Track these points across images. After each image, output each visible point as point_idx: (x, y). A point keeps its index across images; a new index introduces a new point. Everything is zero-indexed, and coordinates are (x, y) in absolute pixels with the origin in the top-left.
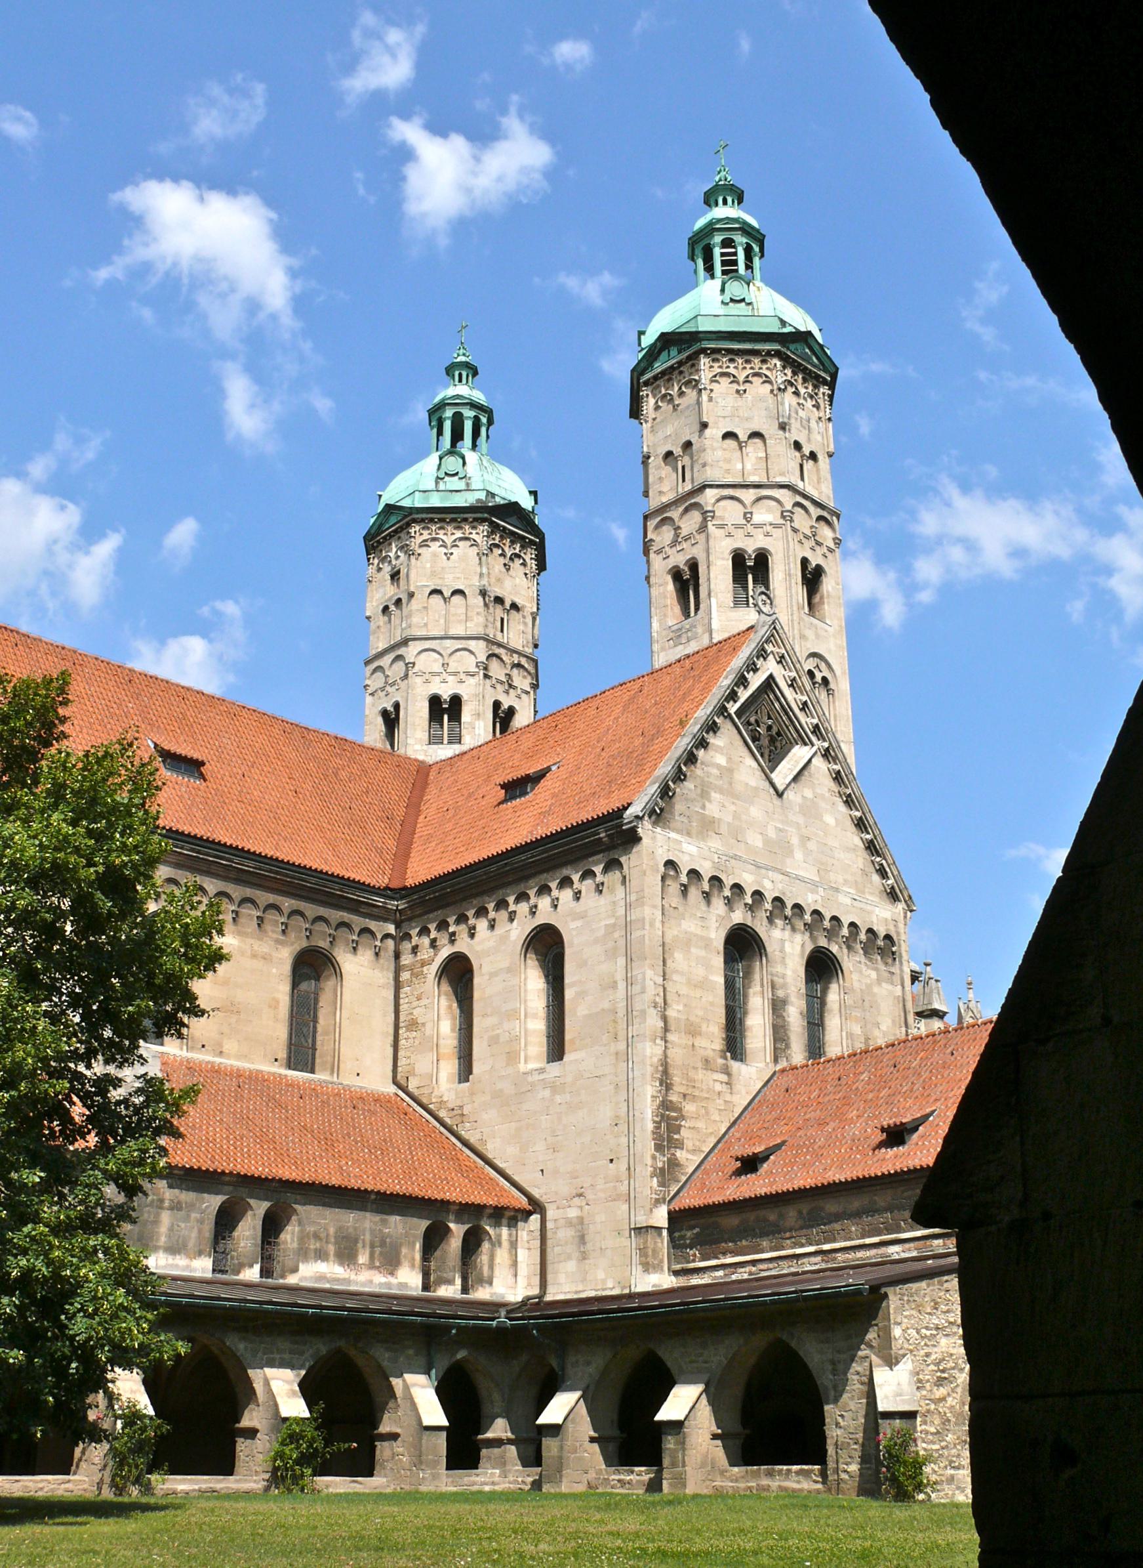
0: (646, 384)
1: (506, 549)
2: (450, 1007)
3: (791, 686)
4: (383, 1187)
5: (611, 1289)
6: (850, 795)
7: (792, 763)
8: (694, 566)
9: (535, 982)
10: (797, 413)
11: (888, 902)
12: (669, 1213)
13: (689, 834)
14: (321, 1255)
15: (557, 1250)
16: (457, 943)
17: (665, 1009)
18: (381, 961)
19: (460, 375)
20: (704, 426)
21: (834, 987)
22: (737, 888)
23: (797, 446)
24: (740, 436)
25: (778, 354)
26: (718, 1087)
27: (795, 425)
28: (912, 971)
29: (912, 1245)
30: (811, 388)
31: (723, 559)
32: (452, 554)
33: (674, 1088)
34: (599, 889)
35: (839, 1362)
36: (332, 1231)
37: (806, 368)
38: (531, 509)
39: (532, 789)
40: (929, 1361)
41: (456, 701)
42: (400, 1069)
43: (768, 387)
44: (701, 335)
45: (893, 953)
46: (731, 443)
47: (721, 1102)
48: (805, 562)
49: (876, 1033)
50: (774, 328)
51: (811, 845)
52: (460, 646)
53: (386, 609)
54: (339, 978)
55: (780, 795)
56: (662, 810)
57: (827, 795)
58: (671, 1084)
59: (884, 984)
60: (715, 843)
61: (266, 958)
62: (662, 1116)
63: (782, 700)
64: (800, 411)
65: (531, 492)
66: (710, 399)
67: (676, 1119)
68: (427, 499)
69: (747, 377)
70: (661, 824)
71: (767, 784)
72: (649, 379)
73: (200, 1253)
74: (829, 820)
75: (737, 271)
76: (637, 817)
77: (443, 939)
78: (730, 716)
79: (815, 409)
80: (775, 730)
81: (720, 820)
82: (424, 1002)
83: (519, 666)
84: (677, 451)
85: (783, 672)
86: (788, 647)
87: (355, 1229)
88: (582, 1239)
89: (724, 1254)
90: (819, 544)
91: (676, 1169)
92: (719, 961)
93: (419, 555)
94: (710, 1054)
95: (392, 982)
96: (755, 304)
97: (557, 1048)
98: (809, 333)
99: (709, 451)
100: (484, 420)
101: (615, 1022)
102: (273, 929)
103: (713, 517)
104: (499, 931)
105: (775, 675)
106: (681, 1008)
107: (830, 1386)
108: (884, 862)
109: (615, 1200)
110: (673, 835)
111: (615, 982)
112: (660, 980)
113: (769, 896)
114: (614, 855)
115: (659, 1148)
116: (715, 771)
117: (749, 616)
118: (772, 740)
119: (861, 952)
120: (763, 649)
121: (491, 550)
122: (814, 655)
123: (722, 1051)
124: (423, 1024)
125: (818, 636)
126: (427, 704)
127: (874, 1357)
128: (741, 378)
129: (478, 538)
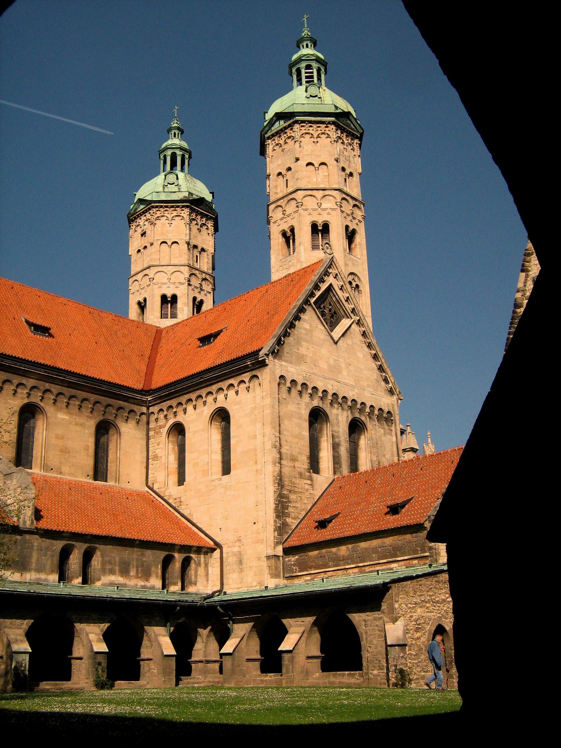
0: (269, 138)
1: (199, 221)
2: (174, 448)
3: (341, 289)
4: (142, 538)
5: (255, 586)
6: (370, 343)
7: (341, 327)
8: (292, 230)
9: (216, 436)
10: (343, 153)
11: (389, 394)
12: (283, 549)
13: (291, 363)
14: (112, 572)
15: (228, 567)
16: (177, 417)
17: (280, 449)
18: (140, 426)
19: (175, 133)
20: (297, 160)
21: (363, 437)
22: (315, 388)
23: (343, 169)
24: (315, 165)
25: (333, 123)
27: (342, 159)
28: (401, 429)
29: (403, 563)
30: (350, 140)
31: (307, 226)
32: (172, 223)
33: (286, 488)
34: (248, 389)
35: (368, 620)
36: (117, 559)
37: (348, 130)
38: (211, 201)
39: (214, 341)
40: (412, 619)
42: (149, 479)
43: (329, 139)
44: (295, 114)
45: (392, 420)
46: (310, 167)
47: (308, 494)
48: (347, 227)
49: (384, 459)
50: (332, 110)
51: (351, 368)
52: (176, 270)
54: (119, 435)
55: (336, 343)
56: (278, 350)
57: (359, 343)
58: (284, 485)
59: (387, 436)
60: (304, 367)
61: (82, 425)
62: (279, 501)
63: (337, 296)
64: (345, 152)
65: (211, 193)
66: (300, 147)
67: (286, 502)
68: (159, 196)
70: (277, 358)
71: (329, 337)
72: (270, 136)
73: (52, 572)
74: (360, 355)
75: (313, 81)
76: (266, 354)
77: (171, 415)
78: (310, 305)
79: (352, 151)
80: (333, 310)
81: (306, 355)
82: (161, 446)
83: (205, 279)
84: (284, 172)
85: (337, 282)
86: (340, 270)
87: (129, 558)
88: (241, 562)
89: (310, 568)
90: (354, 218)
91: (287, 527)
92: (306, 425)
93: (155, 224)
94: (302, 470)
95: (145, 437)
96: (322, 98)
97: (226, 469)
98: (349, 113)
99: (300, 173)
100: (187, 156)
101: (256, 455)
102: (86, 412)
103: (302, 205)
104: (198, 410)
105: (333, 284)
106: (288, 448)
107: (363, 632)
108: (387, 375)
109: (256, 543)
110: (283, 363)
111: (256, 435)
112: (278, 435)
113: (330, 393)
114: (254, 373)
115: (278, 517)
116: (304, 332)
117: (319, 255)
118: (332, 317)
119: (376, 420)
120: (327, 271)
121: (191, 221)
123: (308, 469)
124: (161, 457)
125: (353, 264)
126: (160, 299)
127: (385, 618)
128: (315, 136)
129: (185, 216)
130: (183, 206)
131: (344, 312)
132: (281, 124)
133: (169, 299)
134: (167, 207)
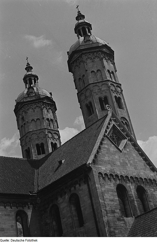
8: (90, 103)
20: (87, 70)
23: (108, 71)
25: (100, 51)
26: (122, 225)
41: (42, 144)
43: (99, 59)
46: (93, 73)
48: (115, 96)
51: (131, 162)
53: (22, 126)
69: (94, 57)
74: (134, 155)
83: (55, 133)
90: (117, 92)
106: (109, 207)
120: (111, 119)
122: (122, 118)
130: (38, 102)
131: (122, 136)
132: (76, 56)
133: (40, 146)
134: (31, 103)
